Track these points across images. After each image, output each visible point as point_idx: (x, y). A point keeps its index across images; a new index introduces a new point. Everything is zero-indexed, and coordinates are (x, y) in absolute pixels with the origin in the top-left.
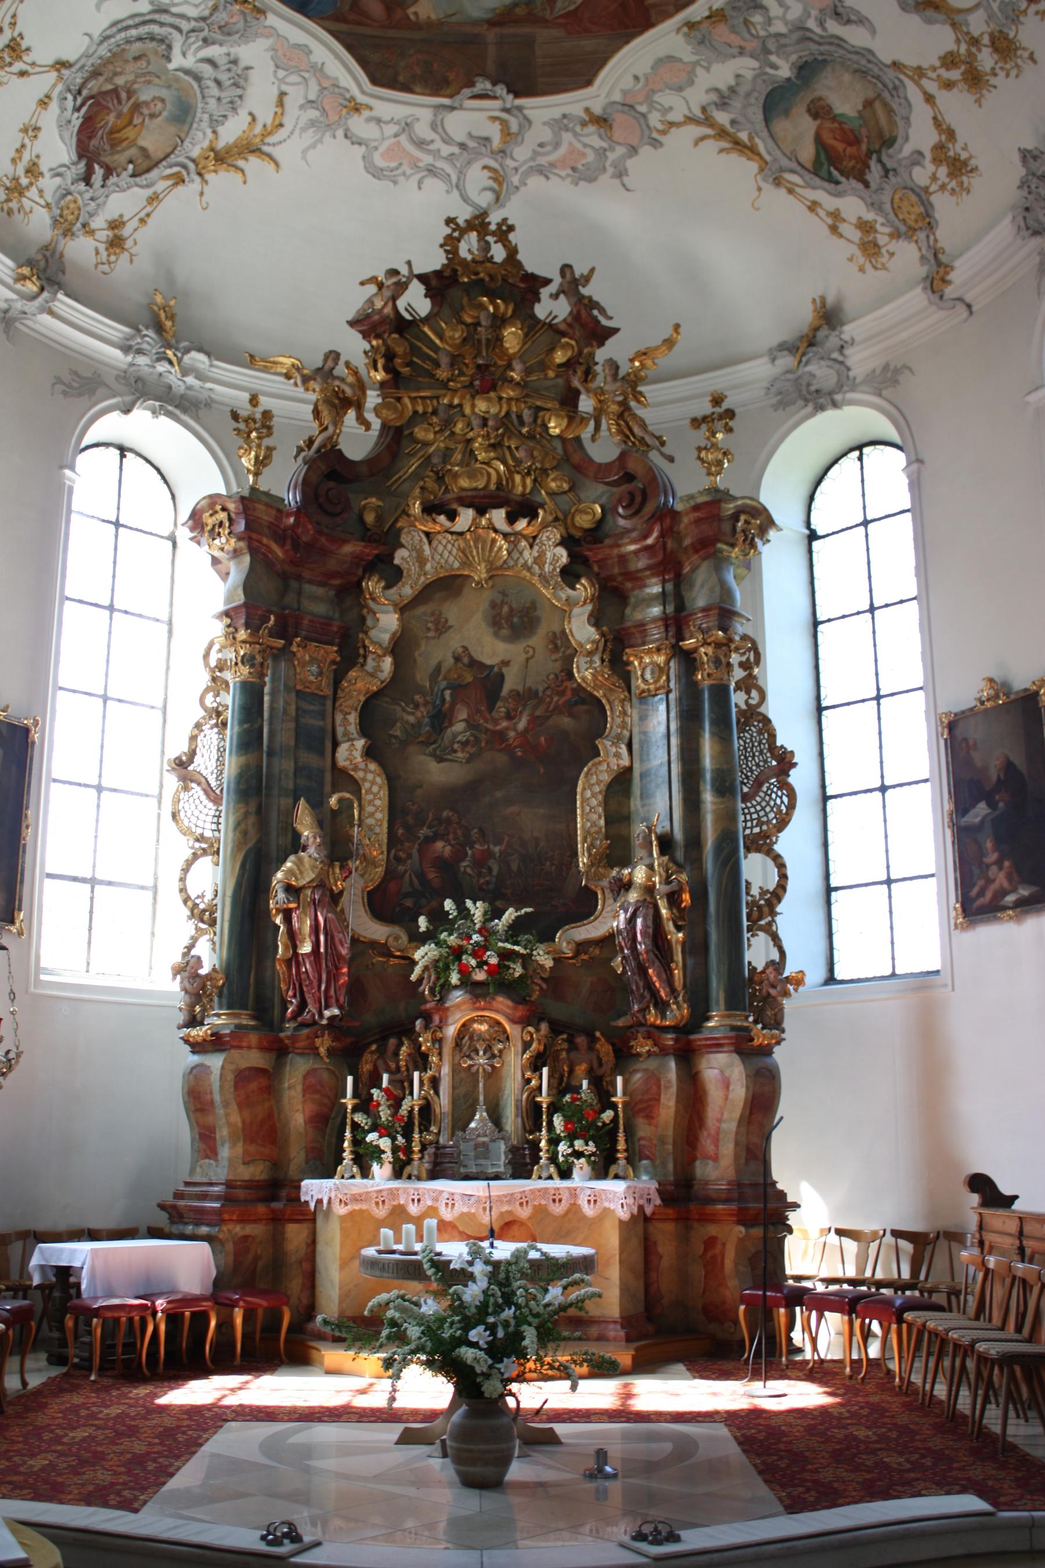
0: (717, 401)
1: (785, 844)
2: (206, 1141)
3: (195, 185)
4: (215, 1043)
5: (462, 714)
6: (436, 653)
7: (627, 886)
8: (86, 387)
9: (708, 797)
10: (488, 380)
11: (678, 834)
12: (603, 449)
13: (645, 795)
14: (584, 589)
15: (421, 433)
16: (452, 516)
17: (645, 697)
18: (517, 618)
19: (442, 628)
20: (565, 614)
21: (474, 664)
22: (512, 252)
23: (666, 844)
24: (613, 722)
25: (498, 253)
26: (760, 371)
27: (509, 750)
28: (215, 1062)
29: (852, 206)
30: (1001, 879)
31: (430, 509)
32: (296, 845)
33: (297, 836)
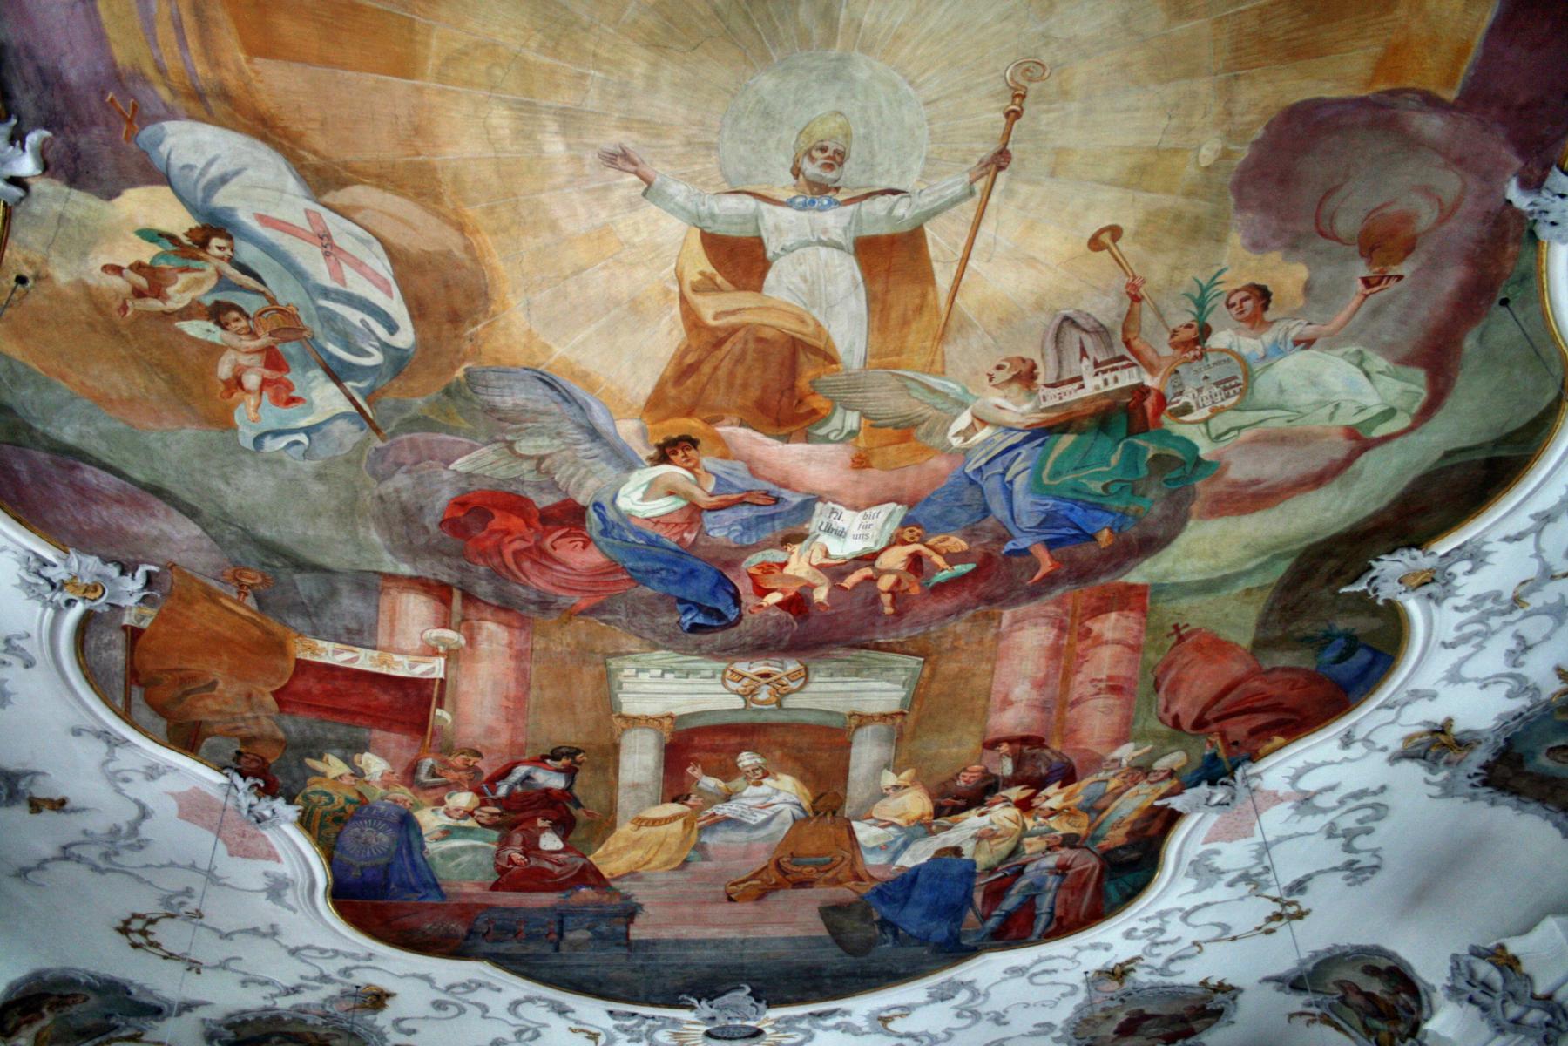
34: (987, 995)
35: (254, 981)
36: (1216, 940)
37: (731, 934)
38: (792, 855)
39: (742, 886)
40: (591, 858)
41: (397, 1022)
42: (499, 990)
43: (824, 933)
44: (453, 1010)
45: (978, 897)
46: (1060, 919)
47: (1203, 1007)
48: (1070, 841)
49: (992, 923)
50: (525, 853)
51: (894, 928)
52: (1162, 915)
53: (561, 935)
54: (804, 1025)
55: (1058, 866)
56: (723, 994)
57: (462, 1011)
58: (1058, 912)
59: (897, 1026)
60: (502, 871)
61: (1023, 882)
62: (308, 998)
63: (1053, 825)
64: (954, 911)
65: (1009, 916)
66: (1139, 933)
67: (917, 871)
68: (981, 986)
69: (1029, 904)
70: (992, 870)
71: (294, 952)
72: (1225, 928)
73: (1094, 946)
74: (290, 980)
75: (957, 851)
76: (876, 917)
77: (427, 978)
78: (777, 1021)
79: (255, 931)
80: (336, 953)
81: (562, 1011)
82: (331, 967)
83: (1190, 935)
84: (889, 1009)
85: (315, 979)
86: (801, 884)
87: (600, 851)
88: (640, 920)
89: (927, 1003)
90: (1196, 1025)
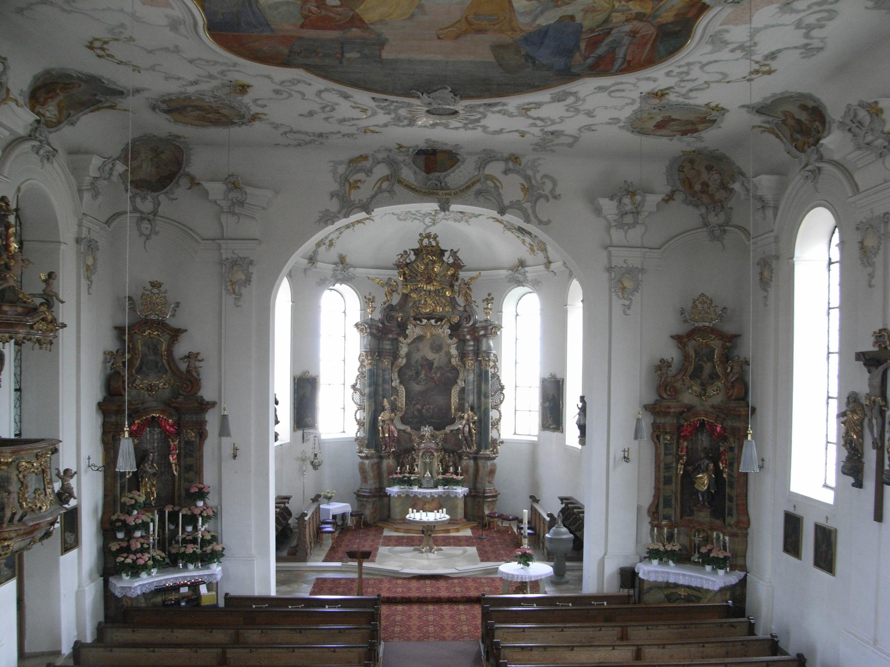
0: (489, 295)
1: (503, 407)
2: (365, 479)
3: (351, 229)
4: (367, 457)
5: (423, 372)
6: (417, 356)
7: (462, 418)
8: (324, 283)
9: (483, 398)
10: (429, 281)
11: (476, 406)
12: (461, 301)
13: (468, 395)
14: (455, 340)
15: (413, 295)
16: (421, 321)
17: (468, 370)
18: (437, 348)
19: (418, 350)
20: (449, 345)
21: (427, 360)
22: (437, 244)
23: (472, 409)
24: (461, 376)
25: (434, 244)
26: (504, 273)
27: (435, 382)
28: (367, 462)
29: (528, 239)
30: (550, 422)
31: (415, 319)
32: (383, 409)
33: (383, 407)
34: (584, 100)
35: (172, 78)
36: (717, 82)
37: (439, 57)
38: (475, 14)
39: (445, 31)
40: (357, 11)
41: (255, 101)
42: (310, 84)
43: (493, 59)
44: (285, 95)
45: (583, 45)
46: (629, 62)
47: (705, 118)
48: (640, 17)
49: (590, 61)
50: (318, 7)
51: (533, 60)
52: (689, 64)
53: (342, 54)
54: (481, 109)
55: (631, 31)
56: (435, 91)
57: (290, 95)
58: (629, 58)
59: (533, 113)
60: (306, 17)
61: (609, 39)
62: (204, 87)
63: (631, 7)
64: (569, 52)
65: (600, 57)
66: (674, 74)
67: (548, 27)
68: (581, 95)
69: (612, 51)
70: (592, 30)
71: (191, 62)
72: (725, 75)
73: (648, 79)
74: (192, 78)
75: (572, 18)
76: (523, 53)
77: (268, 77)
78: (466, 107)
79: (167, 49)
80: (216, 63)
81: (346, 97)
82: (214, 70)
83: (706, 78)
84: (529, 104)
85: (206, 77)
86: (480, 31)
87: (362, 7)
88: (387, 48)
89: (550, 102)
90: (700, 127)
